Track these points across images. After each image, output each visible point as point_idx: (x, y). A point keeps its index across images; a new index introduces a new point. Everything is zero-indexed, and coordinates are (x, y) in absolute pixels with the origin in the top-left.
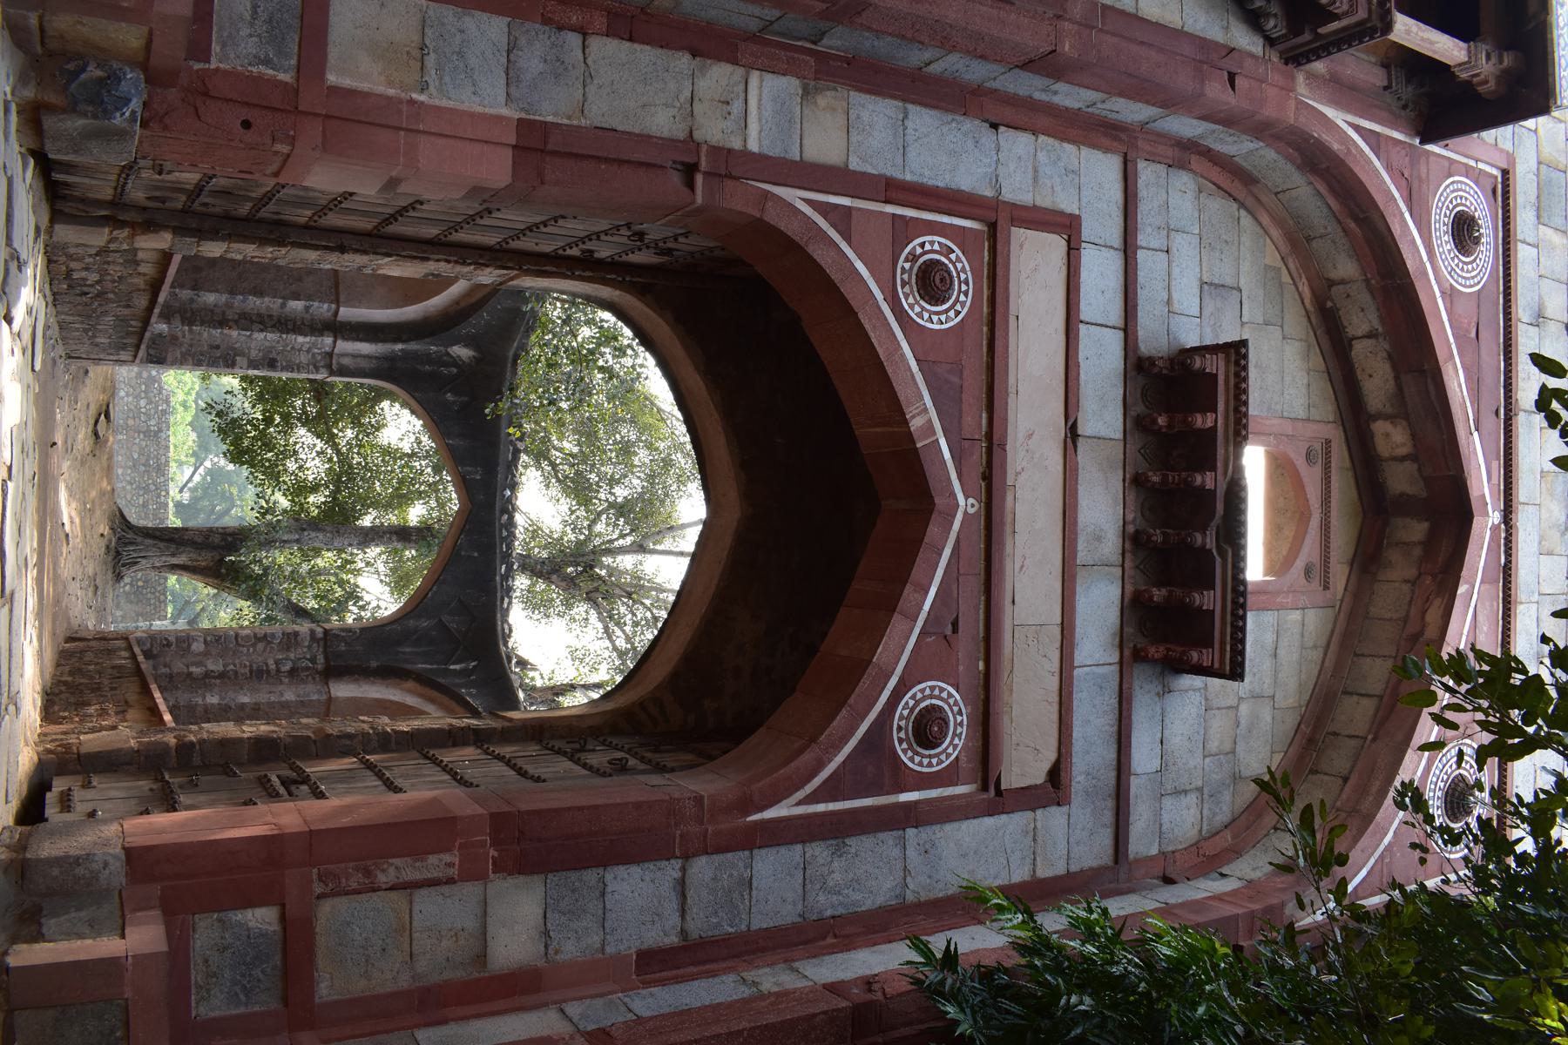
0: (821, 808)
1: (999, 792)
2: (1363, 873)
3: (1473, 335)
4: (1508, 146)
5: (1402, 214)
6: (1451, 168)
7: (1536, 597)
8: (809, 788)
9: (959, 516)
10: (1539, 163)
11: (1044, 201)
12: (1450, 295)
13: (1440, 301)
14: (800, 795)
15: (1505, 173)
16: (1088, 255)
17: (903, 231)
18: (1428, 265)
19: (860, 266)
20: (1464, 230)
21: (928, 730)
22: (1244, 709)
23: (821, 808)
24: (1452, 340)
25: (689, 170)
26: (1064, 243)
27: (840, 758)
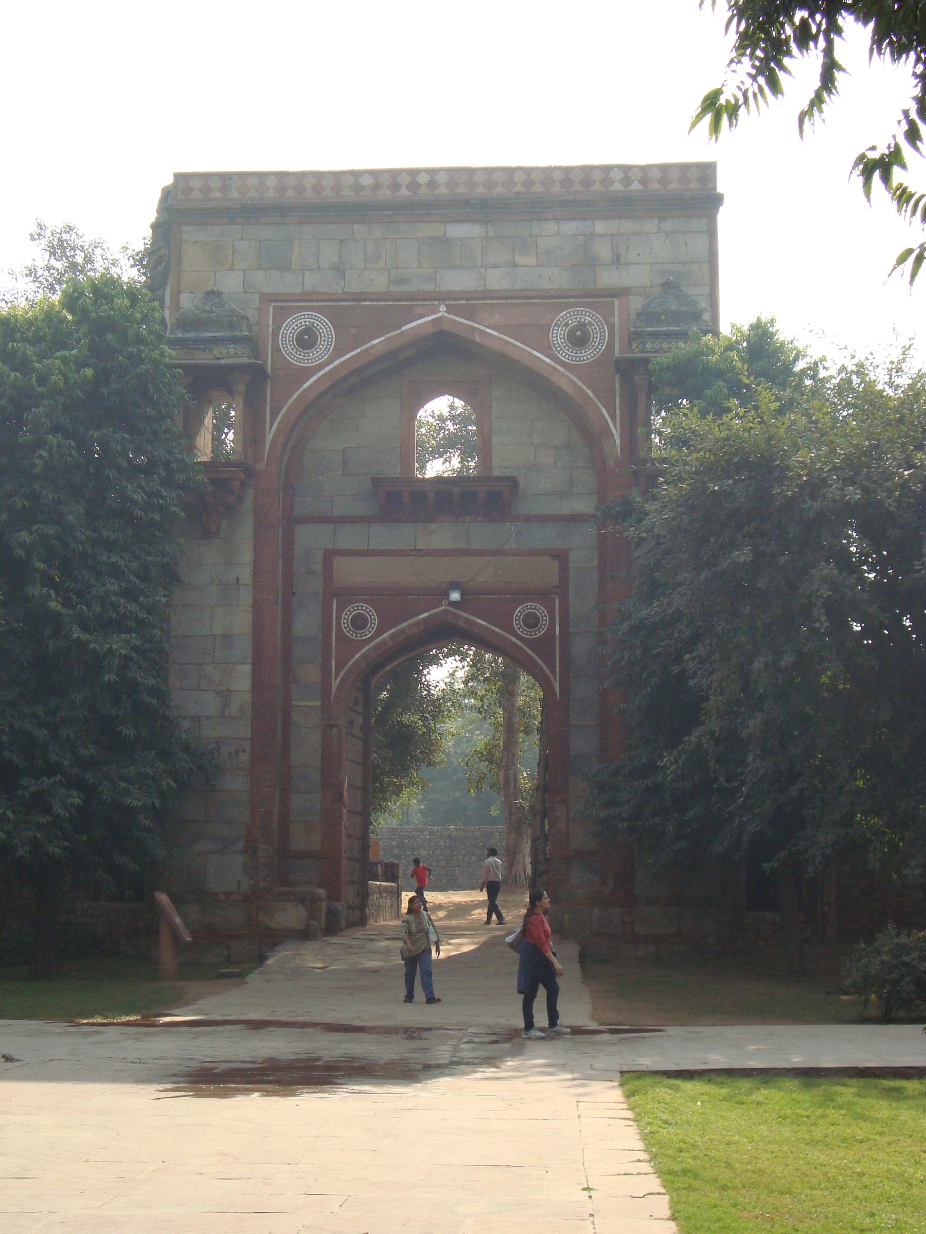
0: (558, 669)
1: (559, 587)
2: (604, 410)
3: (353, 331)
4: (257, 297)
5: (305, 390)
6: (277, 351)
7: (482, 270)
8: (550, 675)
9: (449, 608)
10: (260, 269)
11: (319, 568)
12: (339, 351)
13: (343, 359)
14: (552, 678)
15: (271, 301)
16: (341, 545)
17: (341, 636)
18: (327, 369)
19: (357, 656)
20: (307, 340)
21: (531, 621)
22: (536, 442)
23: (558, 669)
24: (359, 350)
25: (332, 726)
26: (337, 558)
27: (539, 661)
